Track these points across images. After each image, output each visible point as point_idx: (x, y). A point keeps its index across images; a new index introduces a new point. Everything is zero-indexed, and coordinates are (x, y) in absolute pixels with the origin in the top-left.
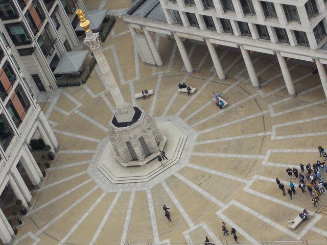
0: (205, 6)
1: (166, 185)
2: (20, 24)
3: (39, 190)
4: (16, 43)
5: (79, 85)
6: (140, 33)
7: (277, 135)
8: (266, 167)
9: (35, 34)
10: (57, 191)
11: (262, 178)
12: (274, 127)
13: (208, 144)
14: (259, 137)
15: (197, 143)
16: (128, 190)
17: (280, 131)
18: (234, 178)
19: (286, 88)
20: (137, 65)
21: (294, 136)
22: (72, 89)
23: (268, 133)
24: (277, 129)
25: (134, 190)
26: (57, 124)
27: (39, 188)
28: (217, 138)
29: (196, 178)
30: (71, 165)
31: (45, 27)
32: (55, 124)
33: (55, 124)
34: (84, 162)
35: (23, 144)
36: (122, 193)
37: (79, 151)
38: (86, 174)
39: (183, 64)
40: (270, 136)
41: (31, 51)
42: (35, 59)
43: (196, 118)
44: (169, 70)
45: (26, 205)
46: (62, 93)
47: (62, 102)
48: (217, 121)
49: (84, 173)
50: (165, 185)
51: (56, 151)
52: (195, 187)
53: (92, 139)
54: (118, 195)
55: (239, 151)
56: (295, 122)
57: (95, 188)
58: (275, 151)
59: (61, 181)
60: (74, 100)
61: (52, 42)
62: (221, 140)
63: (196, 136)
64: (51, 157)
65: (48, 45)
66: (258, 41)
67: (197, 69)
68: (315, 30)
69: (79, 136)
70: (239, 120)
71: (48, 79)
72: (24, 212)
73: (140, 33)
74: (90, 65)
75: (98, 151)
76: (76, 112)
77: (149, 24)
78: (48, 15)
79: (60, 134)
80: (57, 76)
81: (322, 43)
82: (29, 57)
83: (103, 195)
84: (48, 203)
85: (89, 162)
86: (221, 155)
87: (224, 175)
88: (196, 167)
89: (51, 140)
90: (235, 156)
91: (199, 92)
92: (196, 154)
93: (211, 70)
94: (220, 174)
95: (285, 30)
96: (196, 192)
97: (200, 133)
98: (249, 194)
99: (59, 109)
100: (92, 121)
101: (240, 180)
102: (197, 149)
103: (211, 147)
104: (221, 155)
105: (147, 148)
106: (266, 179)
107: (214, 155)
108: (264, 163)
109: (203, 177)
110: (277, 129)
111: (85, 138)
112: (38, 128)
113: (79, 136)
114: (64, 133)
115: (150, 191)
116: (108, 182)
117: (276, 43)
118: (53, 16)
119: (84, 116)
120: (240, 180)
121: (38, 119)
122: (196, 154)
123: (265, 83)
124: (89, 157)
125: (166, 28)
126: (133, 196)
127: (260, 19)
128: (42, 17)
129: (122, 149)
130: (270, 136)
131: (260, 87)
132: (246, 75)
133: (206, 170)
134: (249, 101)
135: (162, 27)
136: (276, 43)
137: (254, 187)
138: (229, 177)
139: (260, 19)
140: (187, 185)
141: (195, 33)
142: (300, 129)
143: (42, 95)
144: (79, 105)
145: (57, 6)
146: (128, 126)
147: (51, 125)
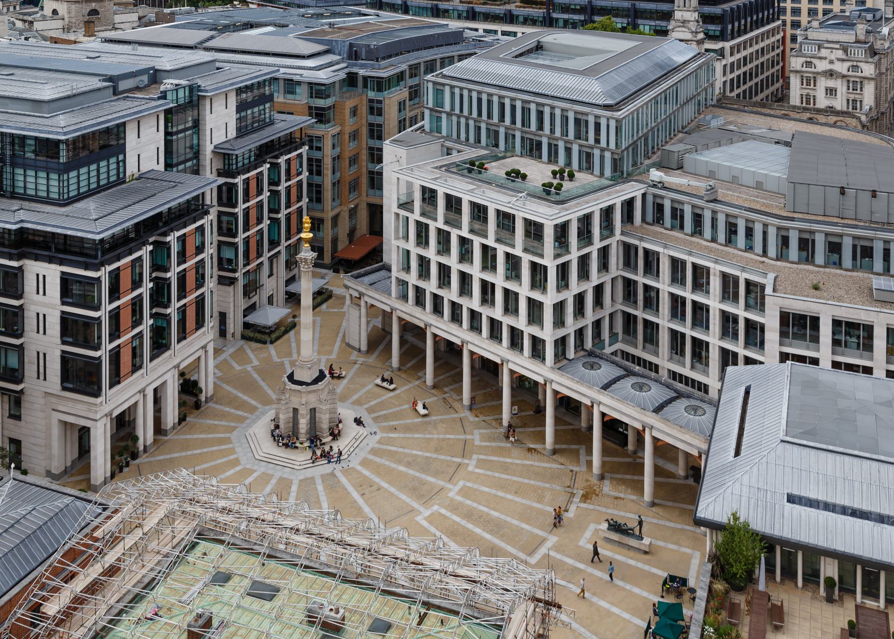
0: (440, 284)
1: (321, 482)
2: (235, 246)
3: (165, 438)
4: (221, 267)
5: (265, 343)
6: (356, 300)
7: (476, 467)
8: (452, 500)
9: (245, 266)
10: (186, 446)
11: (443, 511)
12: (475, 456)
13: (390, 451)
14: (455, 462)
15: (377, 446)
16: (270, 472)
17: (481, 464)
18: (408, 500)
19: (501, 419)
20: (338, 344)
21: (497, 475)
22: (254, 345)
23: (466, 461)
24: (479, 460)
25: (278, 474)
26: (221, 374)
27: (166, 436)
28: (402, 447)
29: (361, 486)
30: (216, 422)
31: (258, 265)
32: (220, 374)
33: (220, 374)
34: (233, 424)
35: (175, 367)
36: (263, 473)
37: (233, 411)
38: (229, 438)
39: (391, 357)
40: (468, 465)
41: (232, 282)
42: (232, 294)
43: (386, 418)
44: (372, 359)
45: (141, 448)
46: (242, 346)
47: (239, 355)
48: (408, 429)
49: (228, 435)
50: (319, 481)
51: (206, 401)
52: (356, 495)
53: (254, 403)
54: (255, 475)
55: (424, 470)
56: (502, 459)
57: (232, 457)
58: (469, 484)
59: (195, 436)
60: (252, 356)
61: (258, 285)
62: (406, 451)
63: (377, 437)
64: (197, 406)
65: (251, 288)
66: (487, 341)
67: (403, 368)
68: (556, 342)
69: (240, 395)
70: (436, 436)
71: (235, 325)
72: (135, 456)
73: (356, 300)
74: (288, 327)
75: (253, 417)
76: (249, 369)
77: (371, 293)
78: (267, 255)
79: (219, 386)
80: (247, 326)
81: (559, 365)
82: (227, 288)
83: (238, 468)
84: (168, 457)
85: (238, 425)
86: (402, 468)
87: (397, 493)
88: (366, 472)
89: (207, 382)
90: (418, 474)
91: (397, 392)
92: (371, 457)
93: (420, 374)
94: (392, 490)
95: (522, 332)
96: (355, 502)
97: (385, 435)
98: (421, 526)
99: (232, 360)
100: (262, 384)
101: (415, 505)
102: (374, 451)
103: (391, 455)
104: (402, 468)
105: (315, 427)
106: (448, 514)
107: (393, 465)
108: (451, 494)
109: (371, 486)
110: (479, 460)
111: (245, 398)
112: (199, 358)
113: (240, 395)
114: (225, 386)
115: (297, 482)
116: (251, 454)
117: (508, 348)
118: (271, 259)
119: (256, 376)
120: (415, 505)
121: (204, 347)
122: (371, 457)
123: (479, 406)
124: (242, 419)
125: (389, 302)
126: (274, 481)
127: (497, 312)
128: (259, 255)
129: (284, 418)
130: (468, 465)
131: (471, 409)
132: (460, 391)
133: (377, 480)
134: (454, 420)
135: (384, 300)
136: (508, 348)
137: (430, 519)
138: (403, 497)
139: (497, 312)
140: (346, 490)
141: (418, 315)
142: (505, 468)
143: (221, 340)
144: (256, 363)
145: (279, 252)
146: (304, 386)
147: (214, 374)
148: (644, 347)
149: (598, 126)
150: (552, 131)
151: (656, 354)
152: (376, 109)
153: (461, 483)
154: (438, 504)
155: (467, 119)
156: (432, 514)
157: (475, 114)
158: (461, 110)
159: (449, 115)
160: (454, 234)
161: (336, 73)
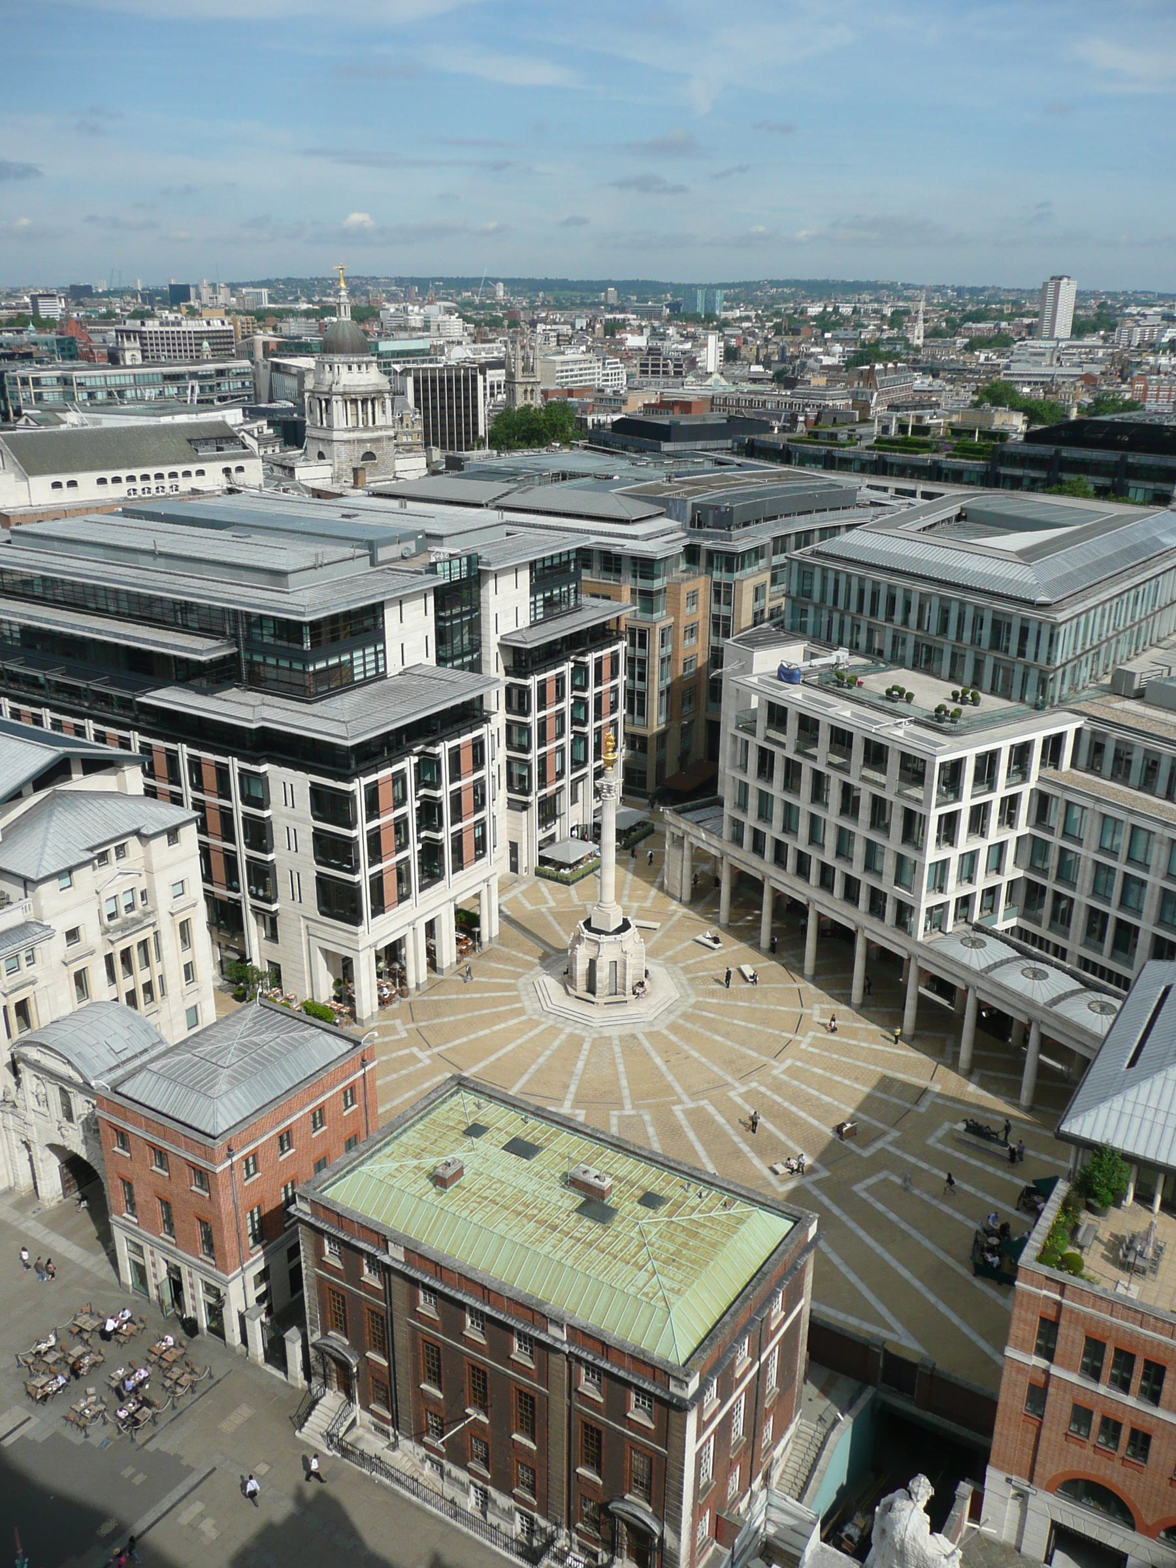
7: (811, 1045)
8: (775, 1078)
11: (762, 1089)
12: (811, 1034)
17: (816, 1042)
18: (721, 1073)
23: (799, 1038)
34: (520, 970)
37: (521, 955)
40: (800, 1042)
41: (525, 806)
42: (525, 821)
49: (512, 981)
50: (617, 1042)
52: (658, 1061)
57: (517, 1005)
58: (799, 1064)
63: (693, 1000)
73: (679, 841)
83: (523, 1018)
102: (684, 1016)
103: (709, 1024)
106: (769, 1093)
118: (575, 782)
130: (800, 1042)
137: (746, 1096)
138: (716, 1069)
141: (754, 864)
148: (1050, 926)
149: (1024, 632)
150: (959, 638)
151: (1065, 935)
152: (723, 593)
153: (789, 1062)
154: (758, 1081)
155: (842, 615)
156: (747, 1092)
157: (853, 608)
158: (835, 603)
159: (818, 608)
160: (807, 766)
161: (670, 545)
